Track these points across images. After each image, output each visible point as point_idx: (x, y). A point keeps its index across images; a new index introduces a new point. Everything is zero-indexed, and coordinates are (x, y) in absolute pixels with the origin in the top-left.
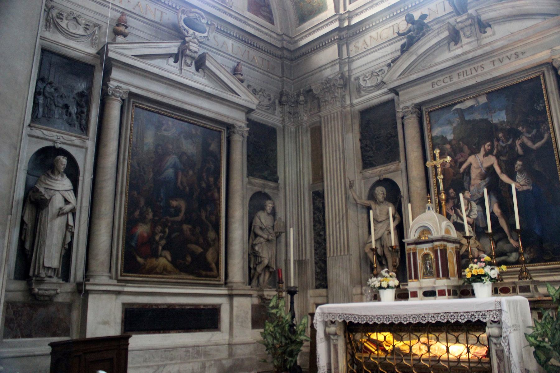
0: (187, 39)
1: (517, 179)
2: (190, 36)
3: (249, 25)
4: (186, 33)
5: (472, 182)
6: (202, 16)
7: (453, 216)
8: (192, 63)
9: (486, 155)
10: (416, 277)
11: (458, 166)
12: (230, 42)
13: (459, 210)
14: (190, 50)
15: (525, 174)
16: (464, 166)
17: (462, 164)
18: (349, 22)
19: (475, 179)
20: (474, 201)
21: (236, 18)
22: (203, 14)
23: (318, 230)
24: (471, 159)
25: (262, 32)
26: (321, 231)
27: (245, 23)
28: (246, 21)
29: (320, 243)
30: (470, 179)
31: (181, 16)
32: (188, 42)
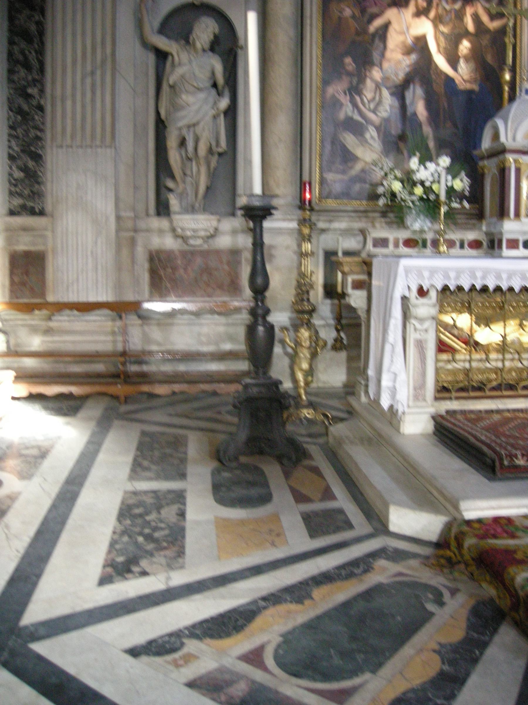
1: (460, 70)
5: (388, 54)
7: (347, 105)
9: (420, 13)
10: (517, 215)
11: (365, 19)
13: (358, 98)
15: (472, 65)
16: (378, 23)
17: (374, 17)
19: (392, 51)
20: (387, 88)
23: (23, 82)
24: (391, 14)
26: (29, 86)
29: (28, 114)
30: (385, 47)
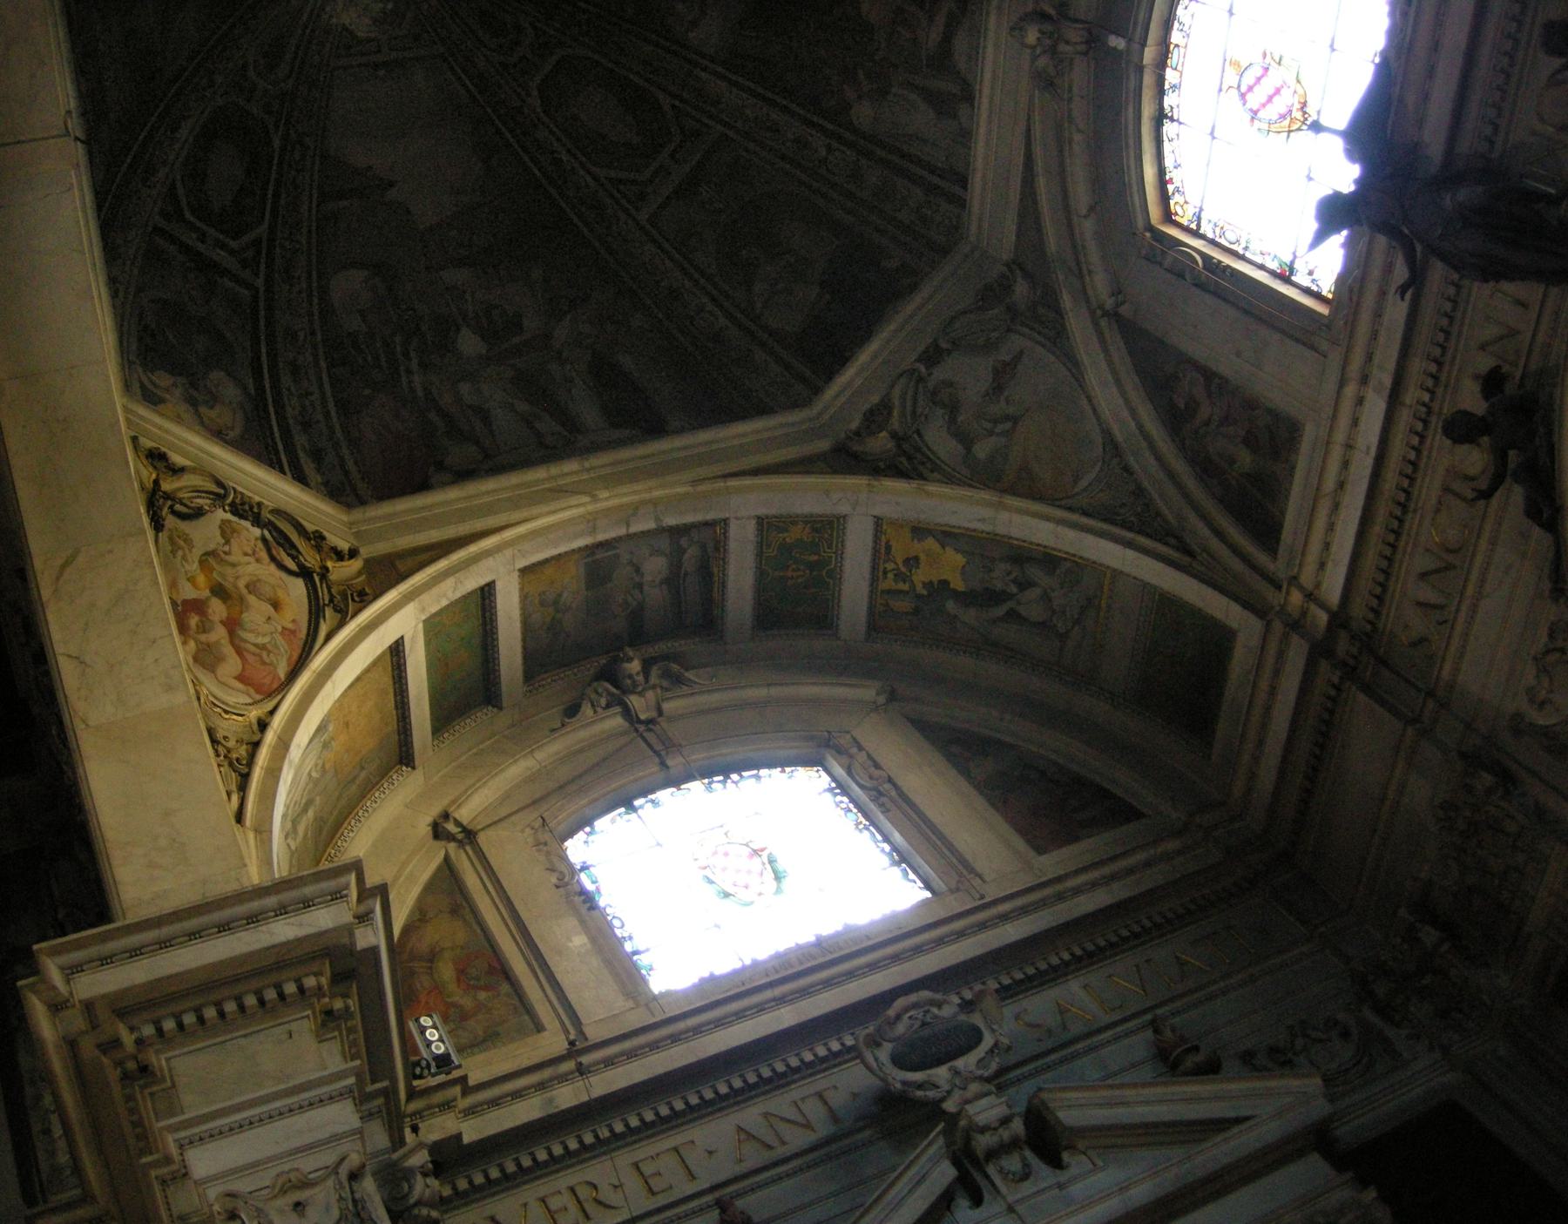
0: (950, 1106)
2: (949, 1092)
3: (1077, 891)
4: (931, 1094)
6: (932, 1003)
8: (1023, 1159)
12: (1074, 990)
14: (983, 1130)
18: (1323, 606)
21: (1024, 911)
22: (925, 994)
25: (1130, 871)
27: (1061, 897)
28: (1059, 887)
31: (876, 1059)
32: (959, 1113)
